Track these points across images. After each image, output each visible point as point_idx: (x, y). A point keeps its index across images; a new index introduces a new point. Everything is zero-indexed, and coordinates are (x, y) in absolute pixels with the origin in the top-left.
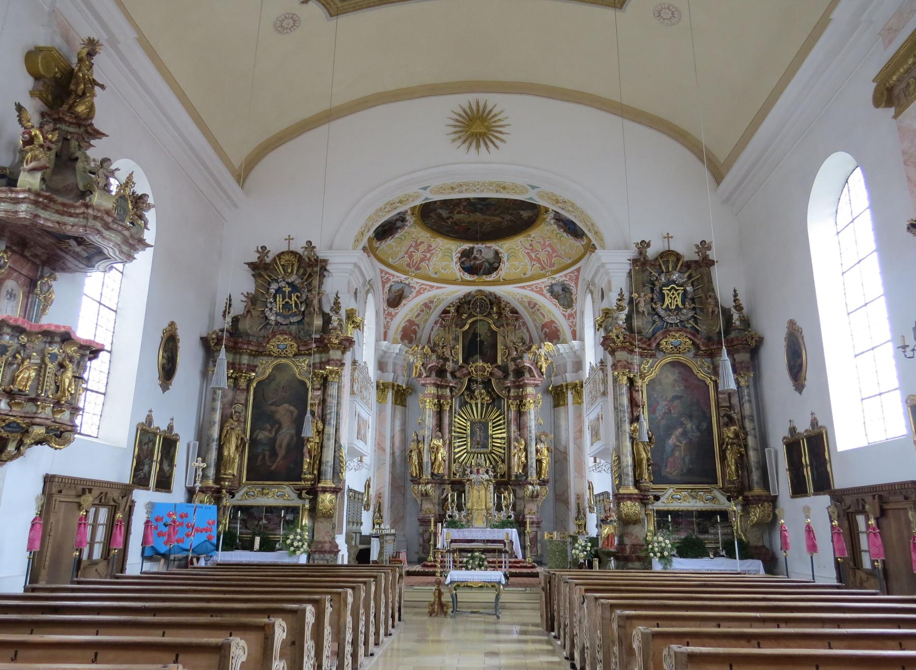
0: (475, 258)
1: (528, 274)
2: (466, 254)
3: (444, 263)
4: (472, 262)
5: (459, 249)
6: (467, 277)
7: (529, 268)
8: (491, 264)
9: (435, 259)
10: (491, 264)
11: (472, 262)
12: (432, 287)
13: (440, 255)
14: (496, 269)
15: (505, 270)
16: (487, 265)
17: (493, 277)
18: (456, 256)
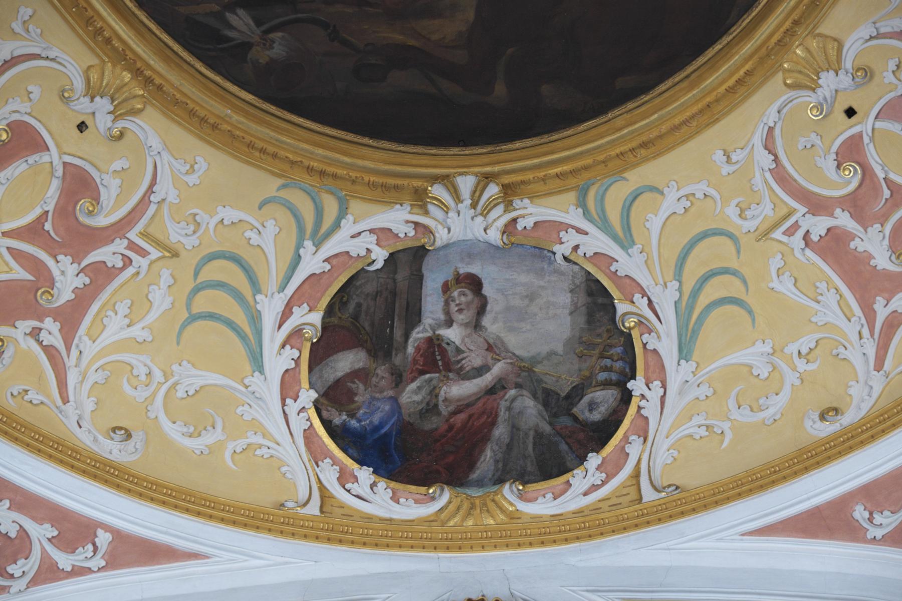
0: (437, 358)
1: (859, 405)
2: (368, 319)
3: (193, 378)
4: (412, 395)
5: (313, 262)
6: (374, 497)
7: (860, 351)
8: (557, 403)
9: (115, 328)
10: (557, 403)
11: (412, 395)
12: (75, 531)
13: (161, 299)
14: (601, 433)
15: (675, 418)
16: (529, 408)
17: (583, 486)
18: (283, 323)
